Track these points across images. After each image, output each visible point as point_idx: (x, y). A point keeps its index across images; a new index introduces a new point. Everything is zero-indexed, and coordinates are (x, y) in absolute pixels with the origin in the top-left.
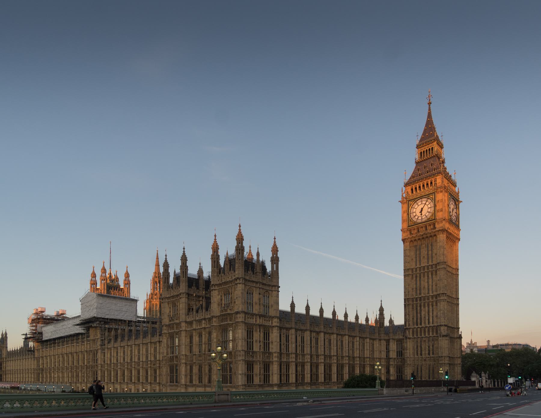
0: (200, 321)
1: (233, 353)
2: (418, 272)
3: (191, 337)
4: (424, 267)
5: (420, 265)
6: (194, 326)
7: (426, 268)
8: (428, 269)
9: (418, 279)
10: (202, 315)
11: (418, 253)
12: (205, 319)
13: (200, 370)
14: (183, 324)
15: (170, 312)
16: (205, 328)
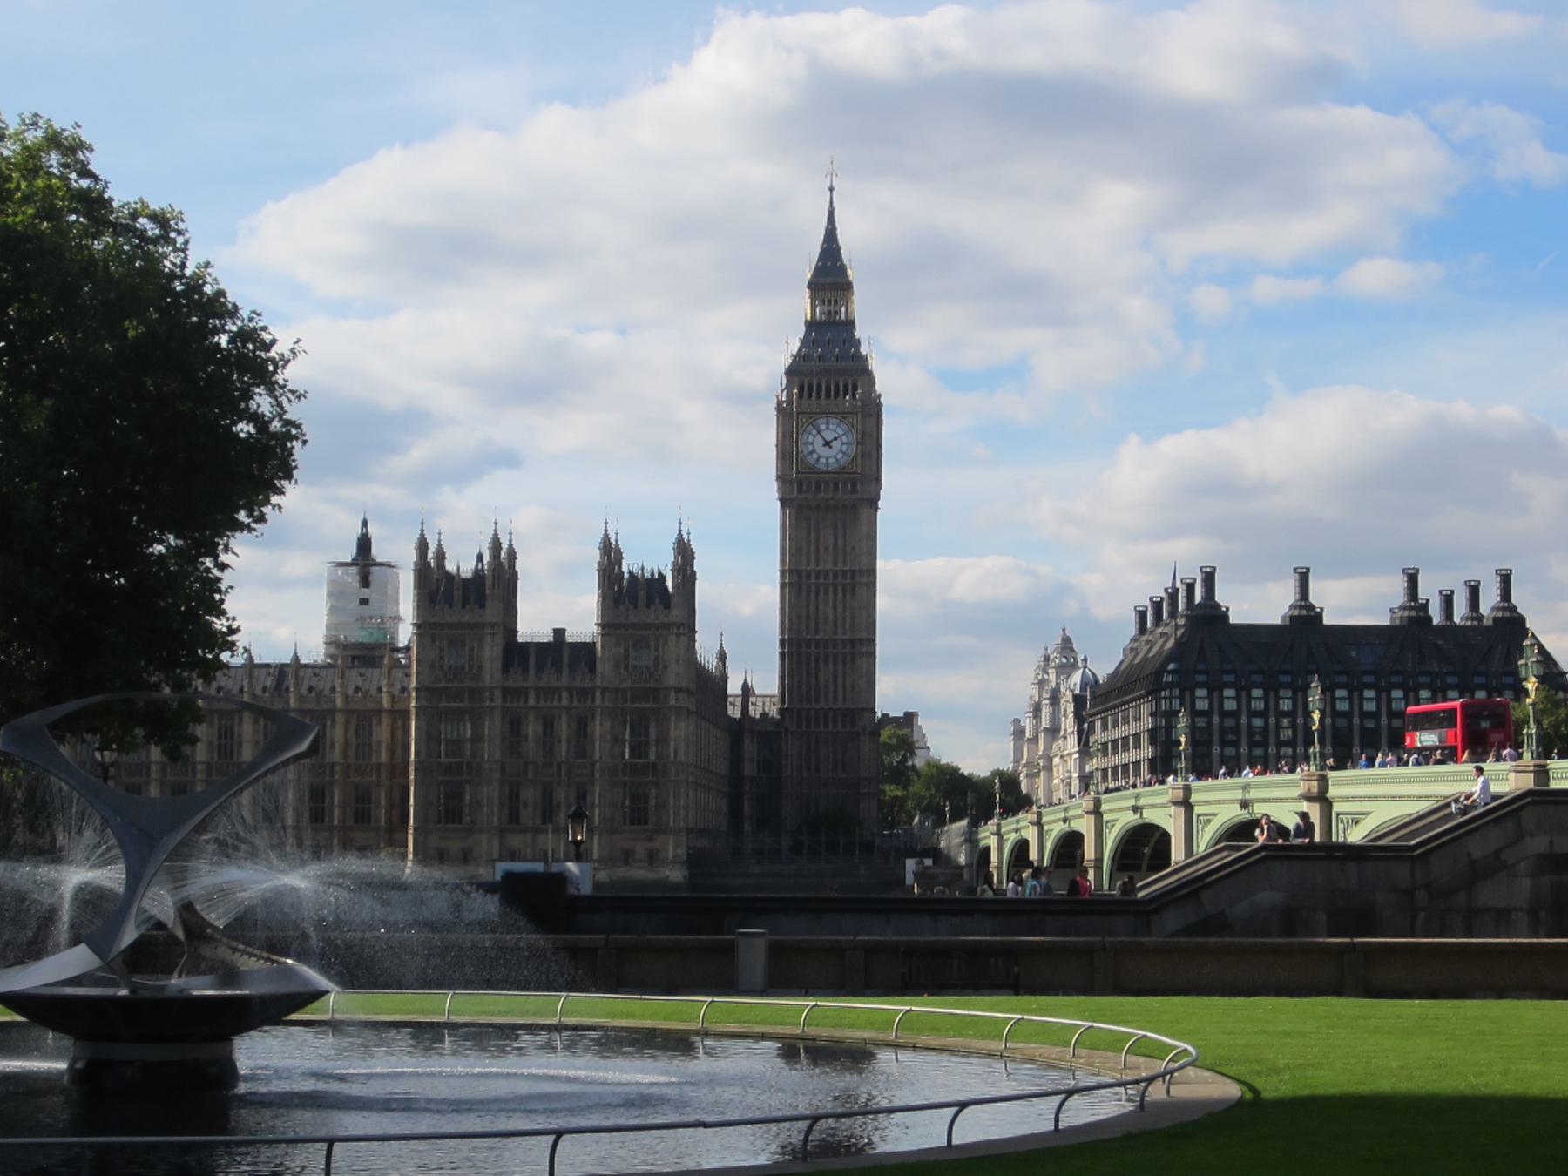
0: (549, 692)
1: (659, 766)
2: (813, 580)
3: (514, 725)
4: (827, 572)
5: (818, 565)
6: (532, 702)
7: (831, 575)
8: (835, 577)
9: (813, 596)
10: (558, 680)
11: (813, 536)
12: (569, 690)
13: (547, 795)
14: (498, 694)
15: (442, 658)
16: (568, 709)
